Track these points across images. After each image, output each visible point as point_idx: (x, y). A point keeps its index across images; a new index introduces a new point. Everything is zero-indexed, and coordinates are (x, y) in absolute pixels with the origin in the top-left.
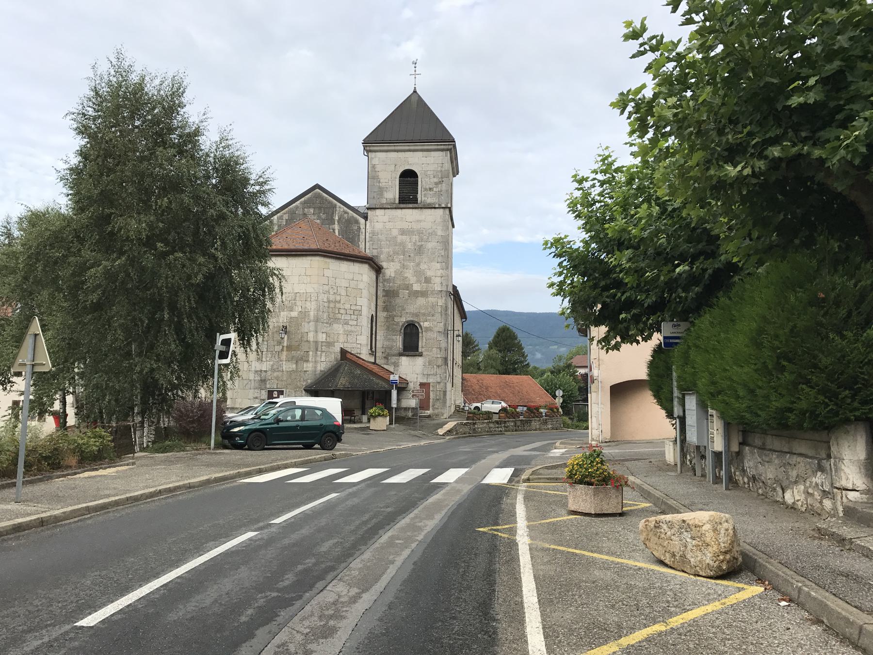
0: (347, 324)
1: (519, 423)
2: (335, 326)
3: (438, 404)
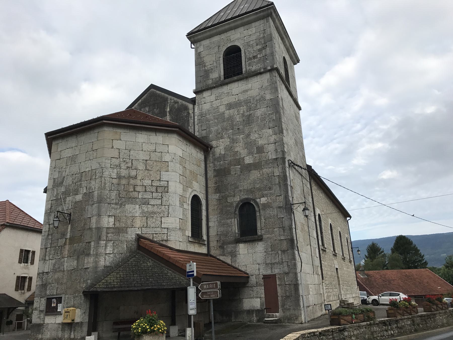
0: (146, 202)
1: (418, 320)
2: (129, 207)
3: (288, 304)
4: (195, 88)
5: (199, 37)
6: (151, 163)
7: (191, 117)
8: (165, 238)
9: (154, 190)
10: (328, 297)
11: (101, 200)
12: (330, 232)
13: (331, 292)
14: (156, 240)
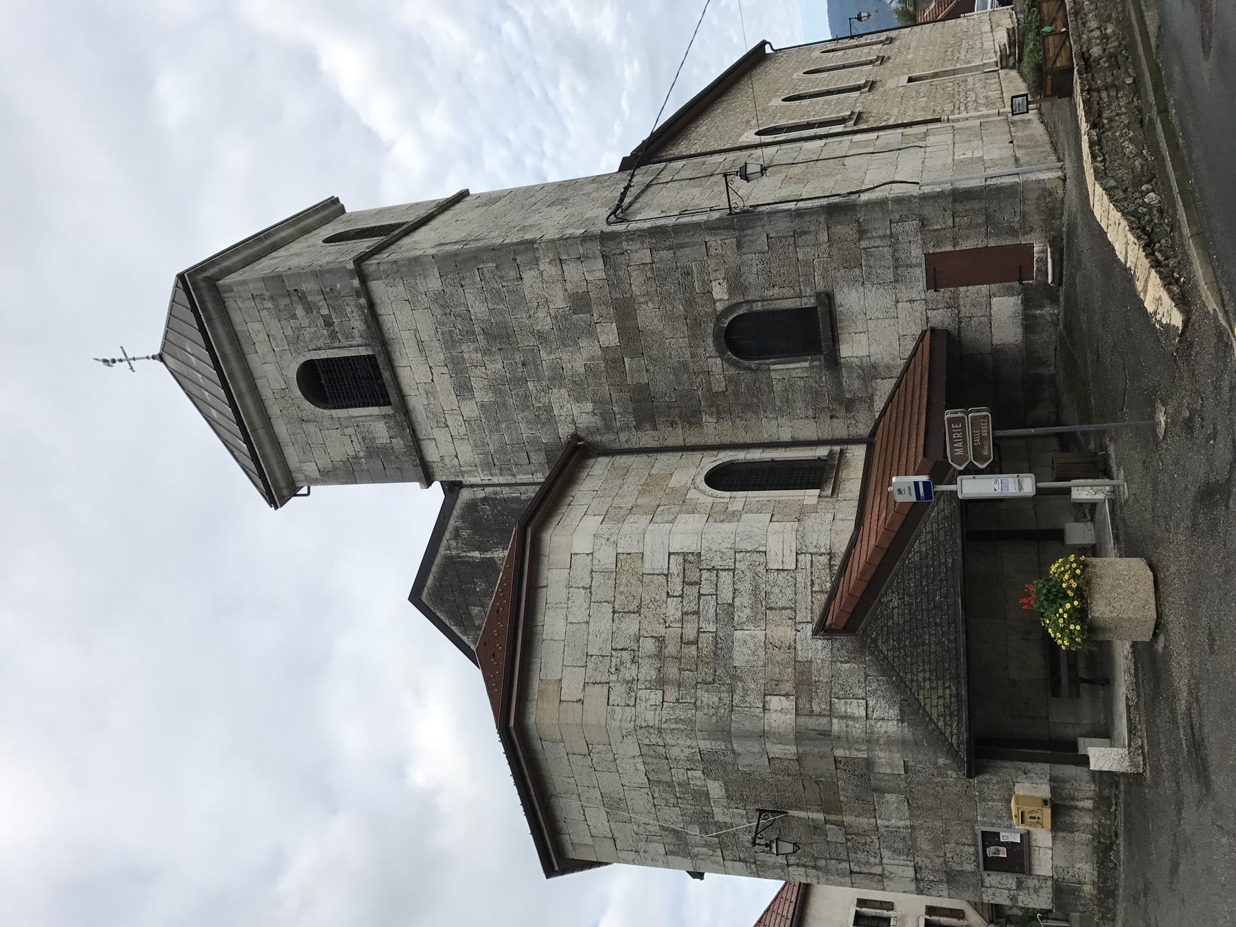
2: (740, 657)
3: (1007, 216)
4: (417, 484)
5: (279, 474)
6: (620, 600)
7: (496, 493)
8: (824, 559)
9: (695, 590)
10: (989, 103)
11: (723, 731)
12: (806, 102)
13: (977, 95)
14: (829, 585)
